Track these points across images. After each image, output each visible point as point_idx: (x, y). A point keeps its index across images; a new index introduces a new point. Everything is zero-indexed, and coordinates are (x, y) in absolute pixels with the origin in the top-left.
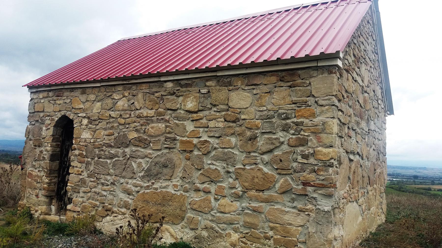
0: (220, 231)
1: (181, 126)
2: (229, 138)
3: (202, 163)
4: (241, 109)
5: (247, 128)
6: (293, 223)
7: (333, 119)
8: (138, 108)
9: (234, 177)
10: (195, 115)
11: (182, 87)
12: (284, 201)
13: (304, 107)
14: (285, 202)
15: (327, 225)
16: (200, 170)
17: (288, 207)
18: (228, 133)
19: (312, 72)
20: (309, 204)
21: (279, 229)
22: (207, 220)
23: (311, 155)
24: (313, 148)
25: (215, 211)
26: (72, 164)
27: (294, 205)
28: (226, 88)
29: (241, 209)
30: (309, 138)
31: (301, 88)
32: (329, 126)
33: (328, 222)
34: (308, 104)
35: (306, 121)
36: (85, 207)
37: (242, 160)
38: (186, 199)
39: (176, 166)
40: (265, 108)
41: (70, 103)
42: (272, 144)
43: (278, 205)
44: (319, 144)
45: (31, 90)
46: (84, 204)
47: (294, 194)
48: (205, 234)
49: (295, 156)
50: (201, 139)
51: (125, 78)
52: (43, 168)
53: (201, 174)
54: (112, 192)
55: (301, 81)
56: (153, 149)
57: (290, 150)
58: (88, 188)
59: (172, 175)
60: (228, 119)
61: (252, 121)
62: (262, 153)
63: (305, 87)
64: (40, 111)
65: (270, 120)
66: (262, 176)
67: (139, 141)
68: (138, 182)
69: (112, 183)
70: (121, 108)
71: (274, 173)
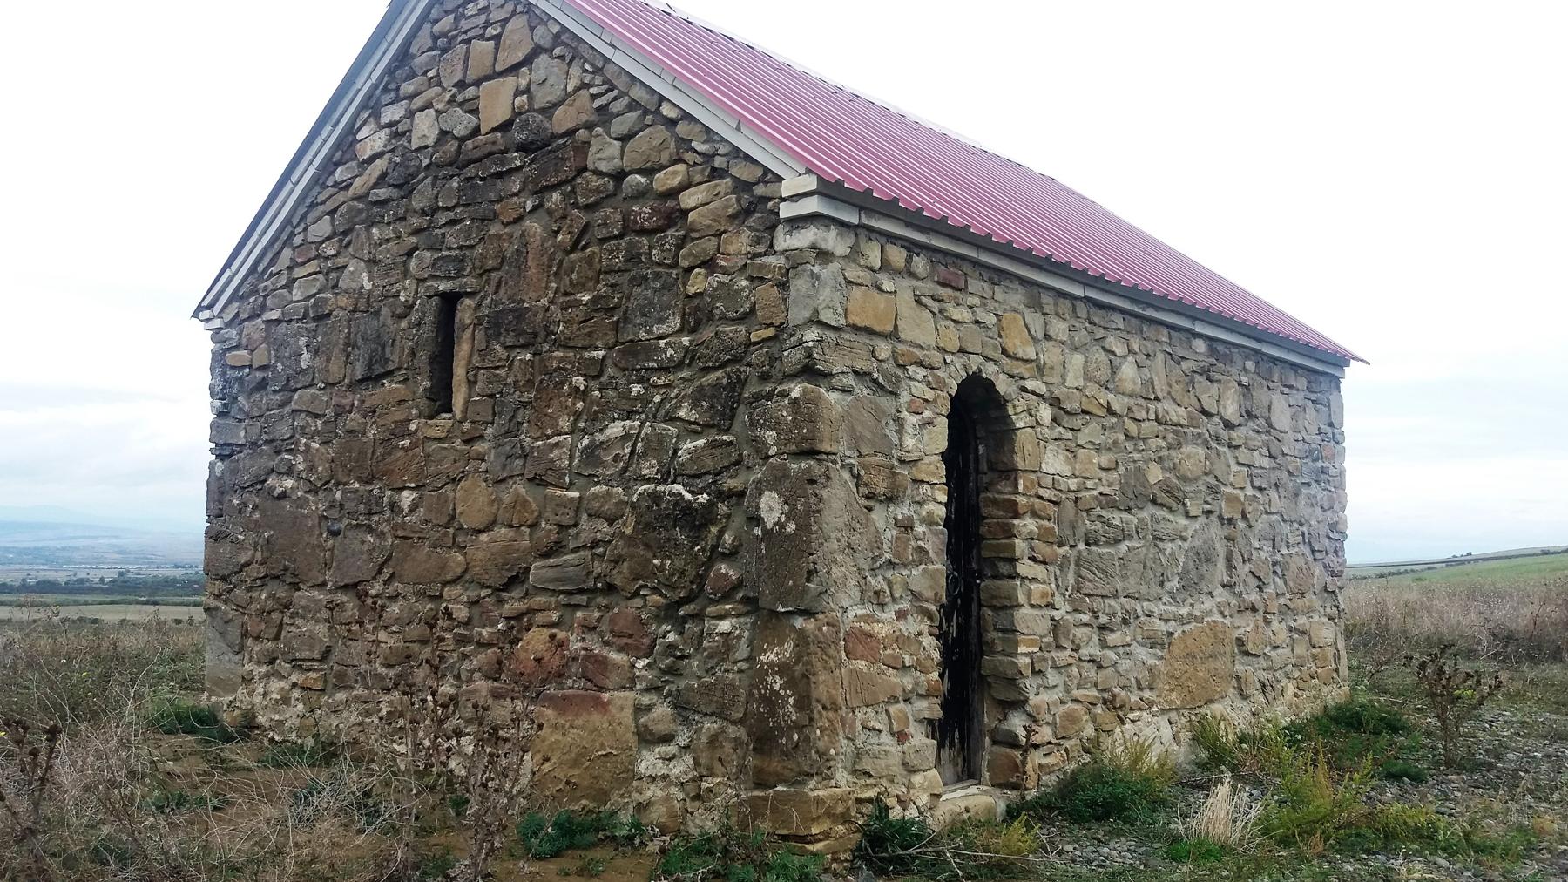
9: (1280, 573)
45: (836, 209)
52: (916, 596)
64: (877, 328)
70: (1128, 387)
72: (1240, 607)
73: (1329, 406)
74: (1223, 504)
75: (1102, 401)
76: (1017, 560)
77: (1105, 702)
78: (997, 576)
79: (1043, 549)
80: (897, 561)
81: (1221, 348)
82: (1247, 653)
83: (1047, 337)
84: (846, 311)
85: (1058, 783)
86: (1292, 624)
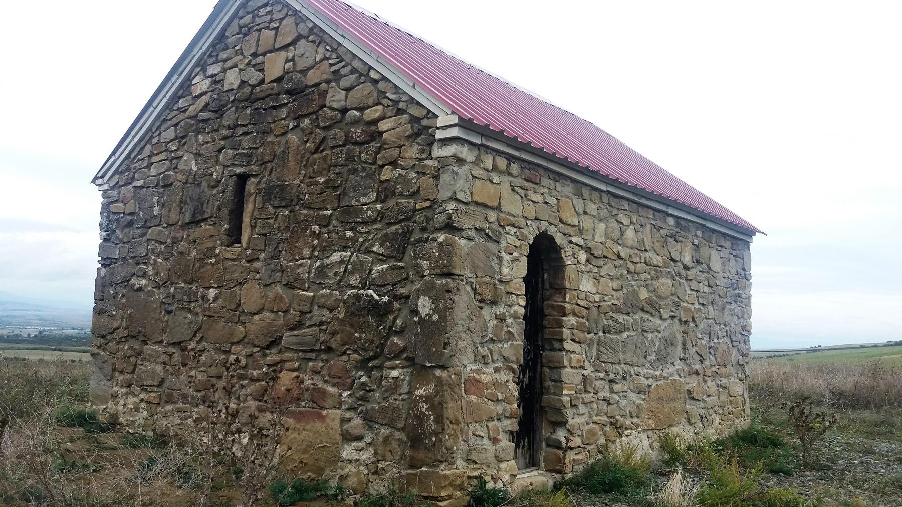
9: (713, 353)
45: (468, 135)
52: (506, 359)
64: (489, 204)
67: (651, 304)
70: (630, 243)
72: (689, 372)
73: (743, 259)
74: (682, 312)
75: (615, 251)
76: (564, 340)
77: (611, 424)
78: (553, 349)
79: (579, 335)
80: (496, 338)
81: (683, 223)
82: (693, 399)
83: (585, 213)
84: (472, 193)
85: (584, 470)
86: (719, 382)
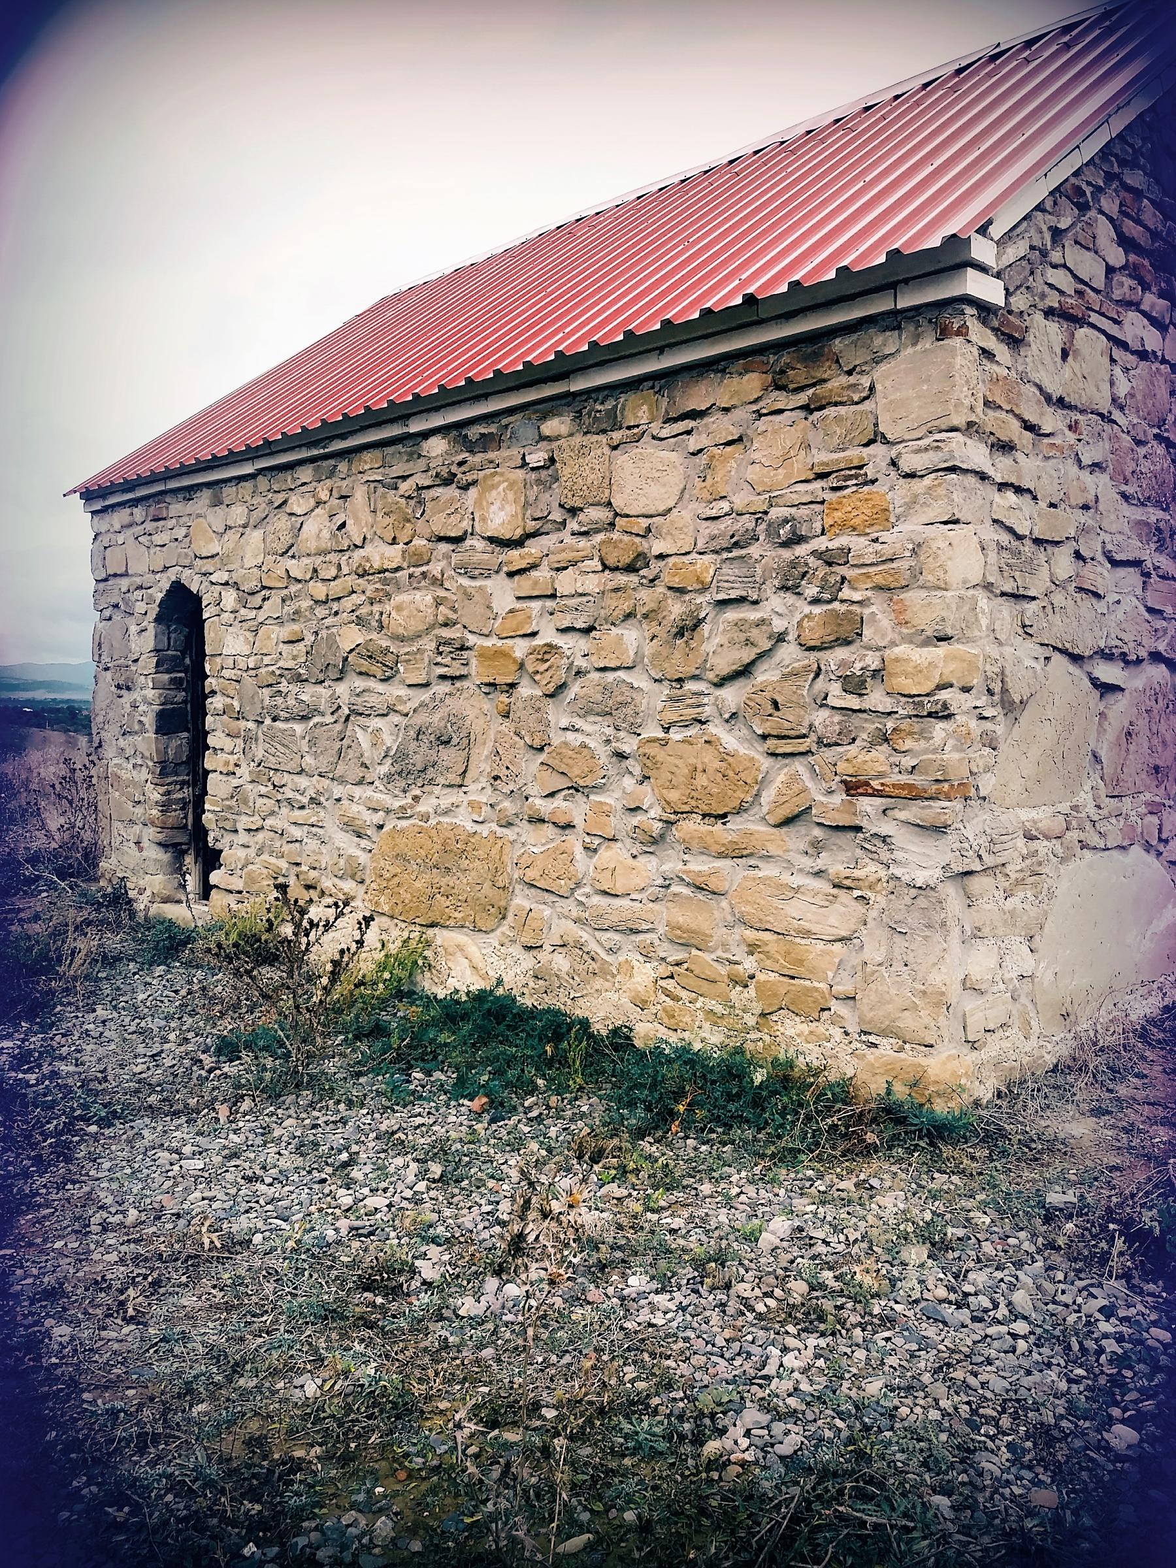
0: (603, 955)
1: (477, 598)
2: (620, 632)
3: (543, 728)
4: (651, 516)
5: (670, 588)
6: (814, 928)
7: (950, 526)
8: (359, 543)
10: (515, 553)
11: (471, 452)
12: (788, 851)
13: (855, 488)
14: (791, 856)
15: (926, 938)
16: (541, 749)
17: (801, 870)
18: (615, 614)
19: (878, 341)
20: (867, 860)
21: (772, 948)
22: (566, 917)
23: (873, 677)
24: (878, 649)
25: (587, 889)
26: (211, 740)
27: (820, 864)
28: (602, 438)
29: (660, 881)
30: (866, 612)
31: (842, 410)
32: (937, 556)
33: (929, 926)
34: (866, 474)
35: (857, 544)
36: (251, 879)
37: (659, 709)
38: (507, 849)
39: (472, 738)
40: (725, 506)
41: (187, 539)
42: (748, 642)
43: (771, 866)
44: (900, 633)
46: (250, 867)
47: (819, 824)
48: (561, 963)
49: (820, 684)
50: (538, 641)
51: (308, 438)
53: (542, 763)
54: (314, 830)
55: (844, 380)
56: (409, 682)
57: (806, 662)
58: (257, 817)
59: (465, 772)
60: (611, 562)
61: (686, 559)
62: (716, 680)
63: (857, 403)
65: (743, 552)
66: (717, 764)
68: (378, 795)
69: (312, 800)
70: (312, 546)
71: (755, 753)
81: (474, 432)
